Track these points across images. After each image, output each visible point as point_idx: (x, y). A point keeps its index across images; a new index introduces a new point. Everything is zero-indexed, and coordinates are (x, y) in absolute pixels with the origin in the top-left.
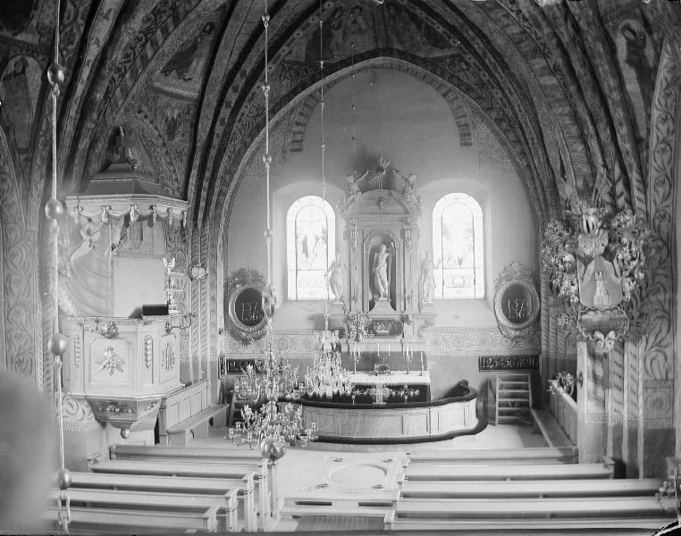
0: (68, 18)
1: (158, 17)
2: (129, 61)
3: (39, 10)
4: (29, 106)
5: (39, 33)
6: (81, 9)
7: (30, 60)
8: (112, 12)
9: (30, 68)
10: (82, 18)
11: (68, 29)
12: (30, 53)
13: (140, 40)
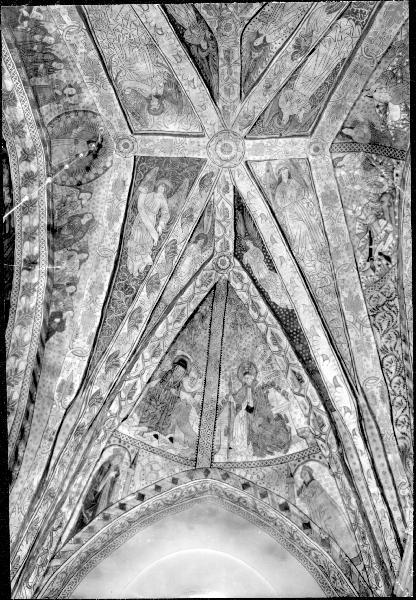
1: (395, 353)
3: (290, 420)
4: (336, 508)
5: (302, 437)
7: (311, 464)
9: (315, 471)
11: (312, 417)
12: (306, 458)
13: (399, 384)
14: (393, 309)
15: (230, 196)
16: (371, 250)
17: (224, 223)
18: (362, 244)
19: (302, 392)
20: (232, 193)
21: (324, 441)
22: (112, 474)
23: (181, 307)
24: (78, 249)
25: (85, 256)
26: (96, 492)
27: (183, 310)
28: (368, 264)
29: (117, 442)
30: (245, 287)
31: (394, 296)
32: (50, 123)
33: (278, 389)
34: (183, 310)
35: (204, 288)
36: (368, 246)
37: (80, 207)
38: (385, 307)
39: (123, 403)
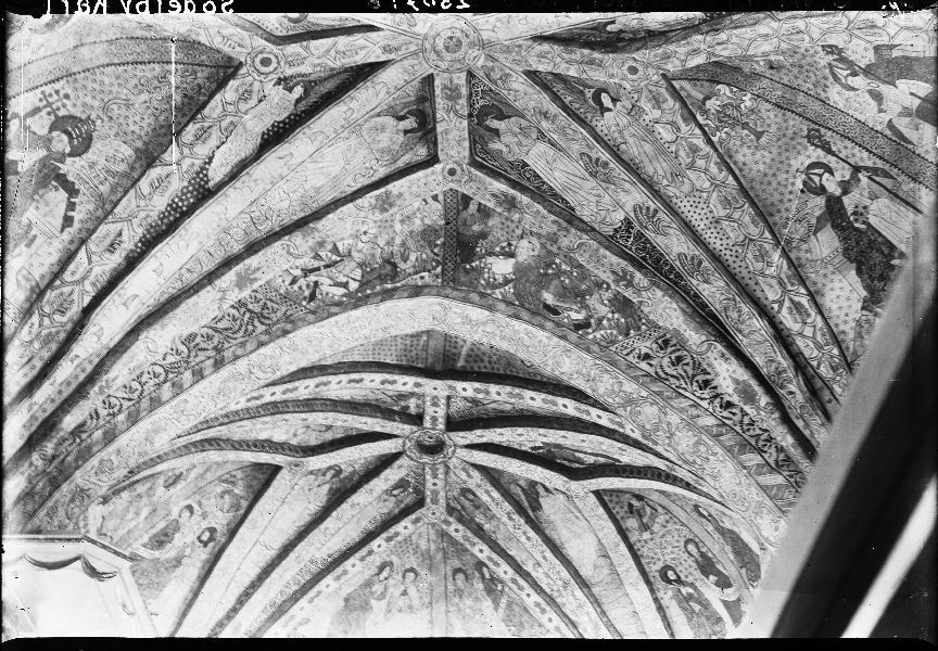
0: (73, 273)
1: (193, 354)
2: (130, 400)
6: (97, 270)
8: (136, 301)
10: (94, 284)
13: (156, 376)
14: (250, 328)
16: (318, 269)
18: (323, 254)
19: (94, 258)
20: (383, 58)
21: (40, 325)
28: (298, 273)
31: (267, 322)
33: (71, 206)
36: (323, 263)
38: (248, 315)
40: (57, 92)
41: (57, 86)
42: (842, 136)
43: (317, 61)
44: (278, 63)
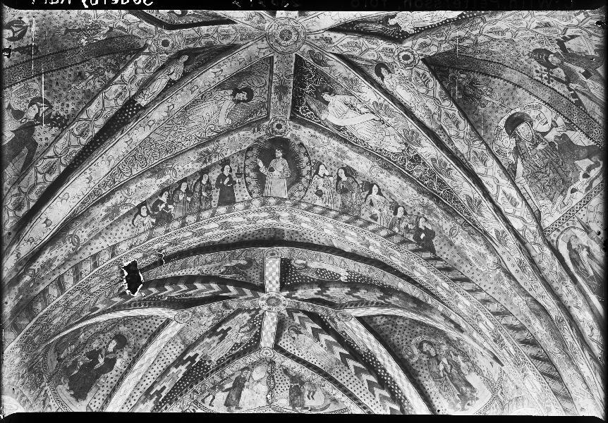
15: (337, 37)
17: (364, 49)
20: (332, 35)
22: (584, 254)
23: (443, 117)
24: (367, 192)
25: (375, 188)
26: (592, 277)
27: (447, 115)
29: (558, 234)
30: (436, 43)
32: (251, 194)
34: (447, 115)
35: (431, 84)
37: (331, 178)
39: (518, 214)
40: (541, 77)
41: (540, 79)
42: (18, 64)
43: (375, 46)
44: (398, 55)
